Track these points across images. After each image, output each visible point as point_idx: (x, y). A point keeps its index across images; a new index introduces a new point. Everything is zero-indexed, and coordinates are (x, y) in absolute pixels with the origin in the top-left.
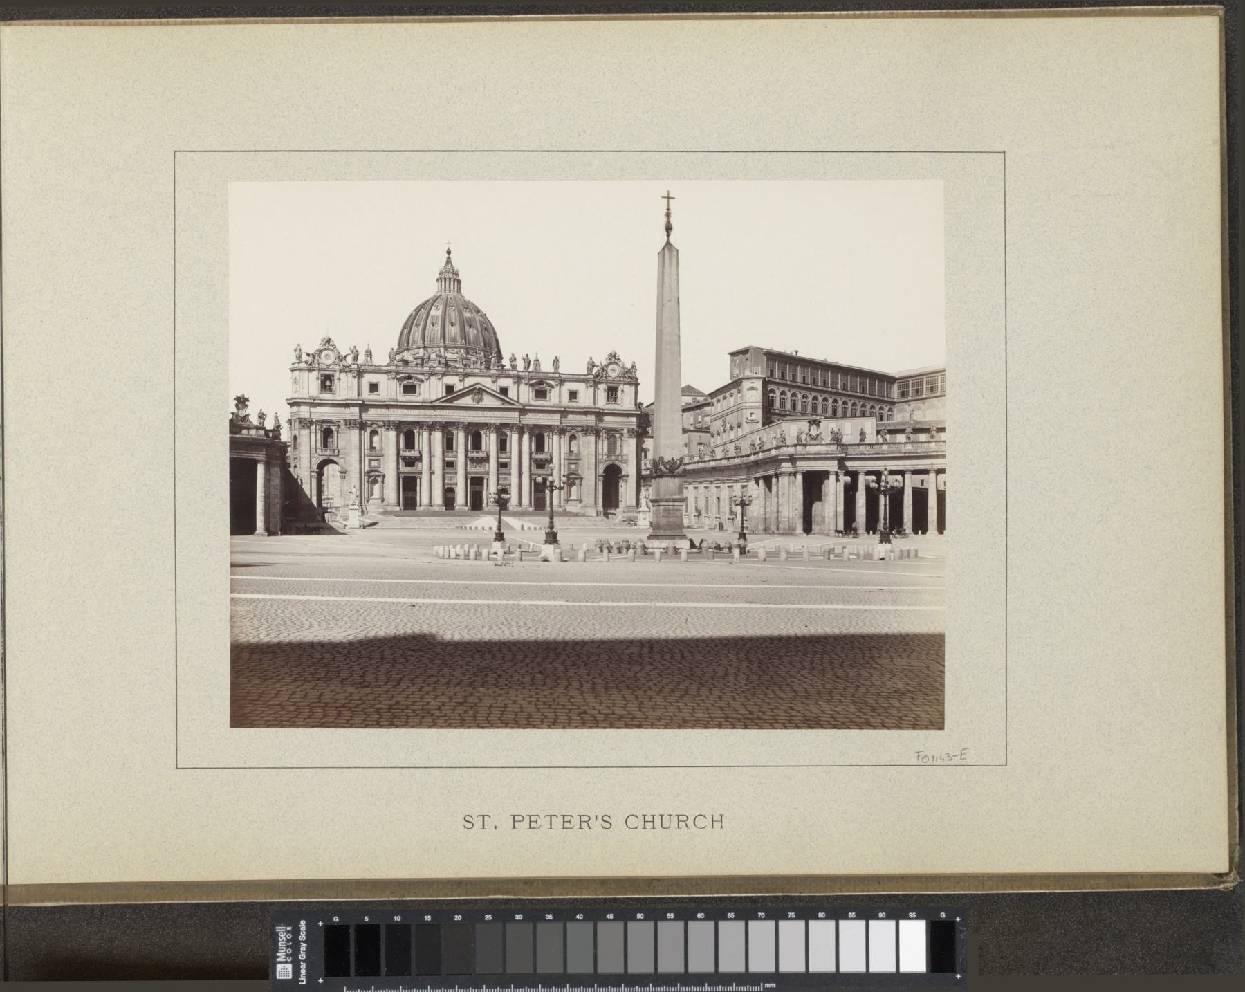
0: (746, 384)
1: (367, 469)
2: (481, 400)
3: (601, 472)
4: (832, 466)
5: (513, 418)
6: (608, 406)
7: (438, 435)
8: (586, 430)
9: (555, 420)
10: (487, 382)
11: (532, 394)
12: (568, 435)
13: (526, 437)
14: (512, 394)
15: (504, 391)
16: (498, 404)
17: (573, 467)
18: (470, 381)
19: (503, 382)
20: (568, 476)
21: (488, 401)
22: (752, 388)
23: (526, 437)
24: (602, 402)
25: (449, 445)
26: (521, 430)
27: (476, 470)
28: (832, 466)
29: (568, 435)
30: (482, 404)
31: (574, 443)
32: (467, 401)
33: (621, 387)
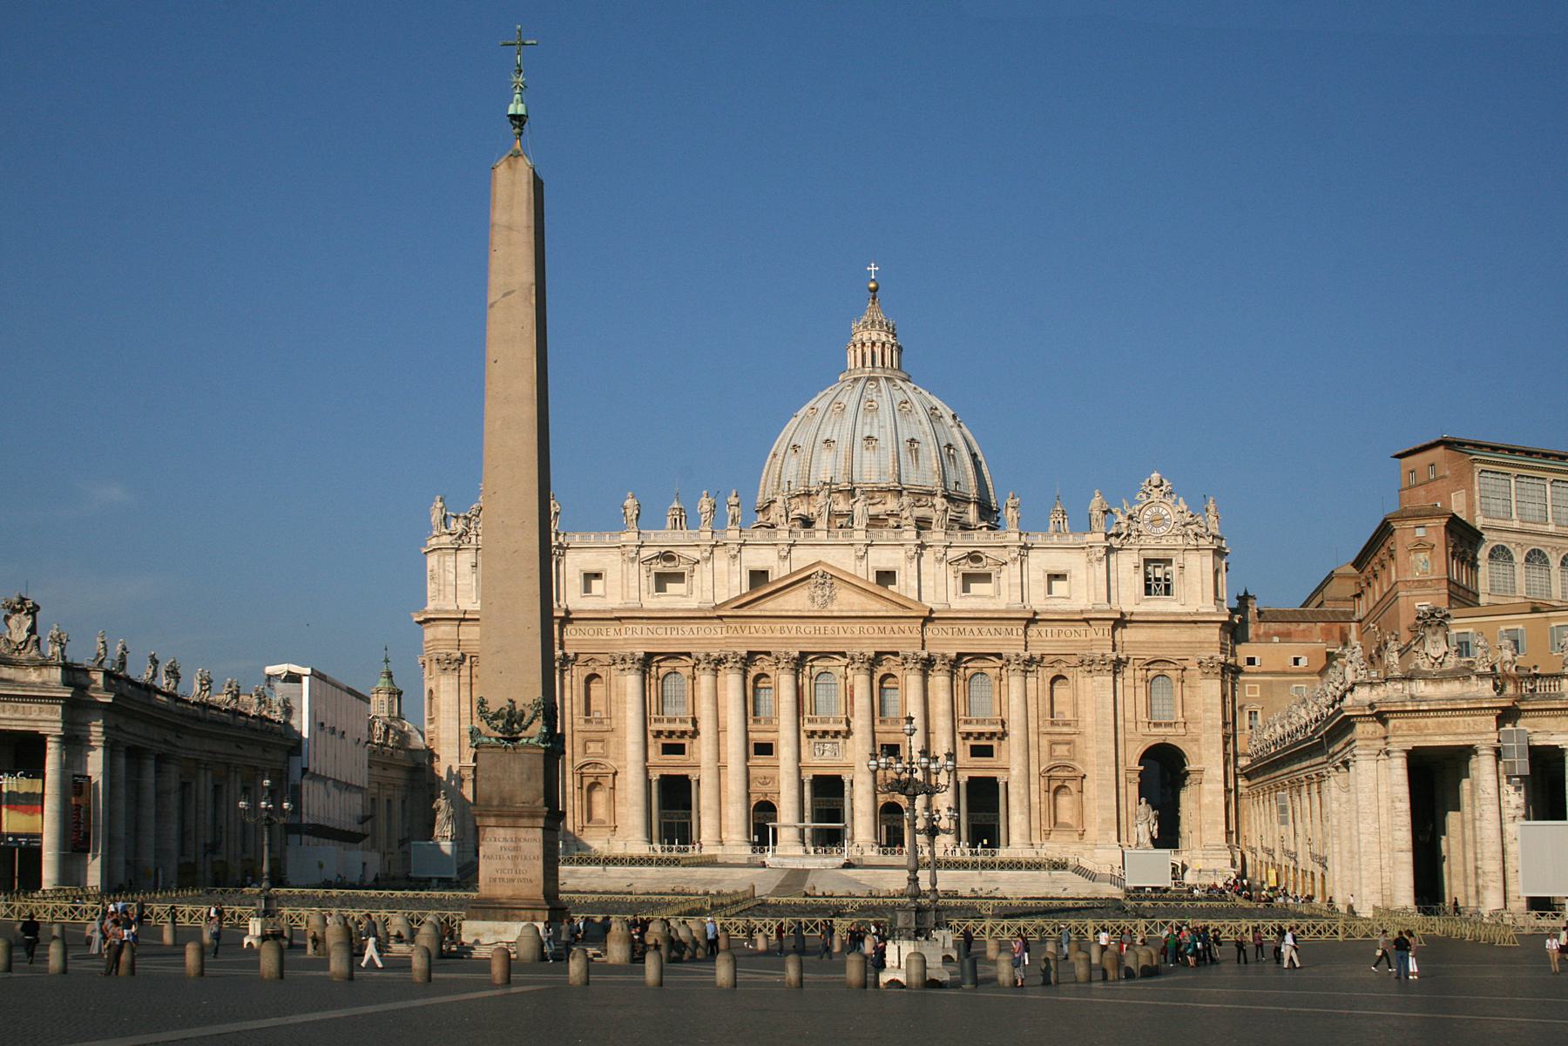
0: (1406, 533)
1: (579, 761)
2: (832, 598)
3: (1134, 762)
4: (1480, 732)
5: (905, 638)
6: (1143, 608)
7: (731, 682)
8: (1088, 664)
9: (1011, 642)
10: (841, 559)
11: (955, 584)
12: (1047, 674)
13: (939, 681)
14: (905, 584)
15: (886, 577)
16: (875, 607)
17: (1061, 750)
18: (803, 557)
19: (883, 558)
20: (1048, 775)
21: (847, 601)
22: (1420, 546)
23: (939, 681)
24: (1130, 597)
25: (752, 708)
26: (927, 665)
27: (822, 760)
28: (1480, 732)
29: (1047, 674)
30: (834, 609)
31: (1061, 691)
32: (796, 601)
33: (1177, 559)
